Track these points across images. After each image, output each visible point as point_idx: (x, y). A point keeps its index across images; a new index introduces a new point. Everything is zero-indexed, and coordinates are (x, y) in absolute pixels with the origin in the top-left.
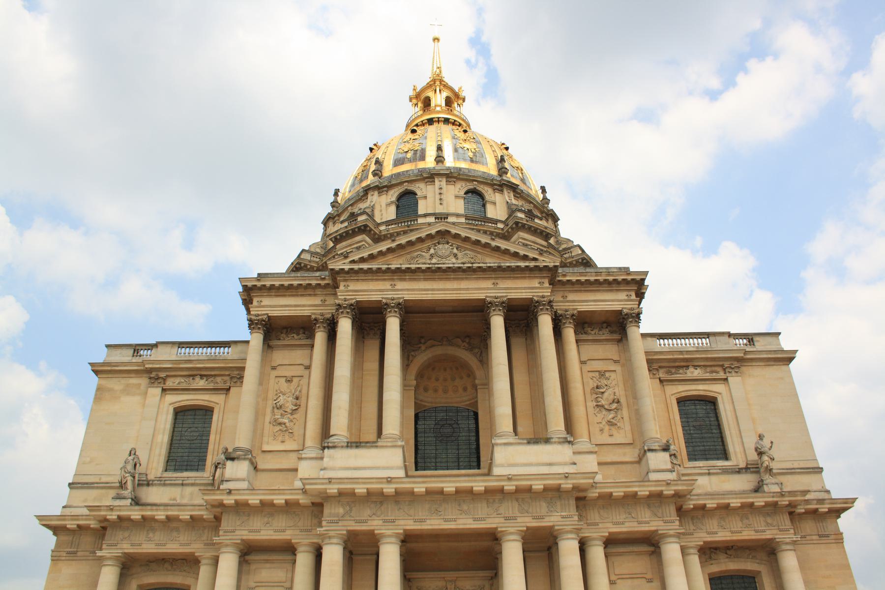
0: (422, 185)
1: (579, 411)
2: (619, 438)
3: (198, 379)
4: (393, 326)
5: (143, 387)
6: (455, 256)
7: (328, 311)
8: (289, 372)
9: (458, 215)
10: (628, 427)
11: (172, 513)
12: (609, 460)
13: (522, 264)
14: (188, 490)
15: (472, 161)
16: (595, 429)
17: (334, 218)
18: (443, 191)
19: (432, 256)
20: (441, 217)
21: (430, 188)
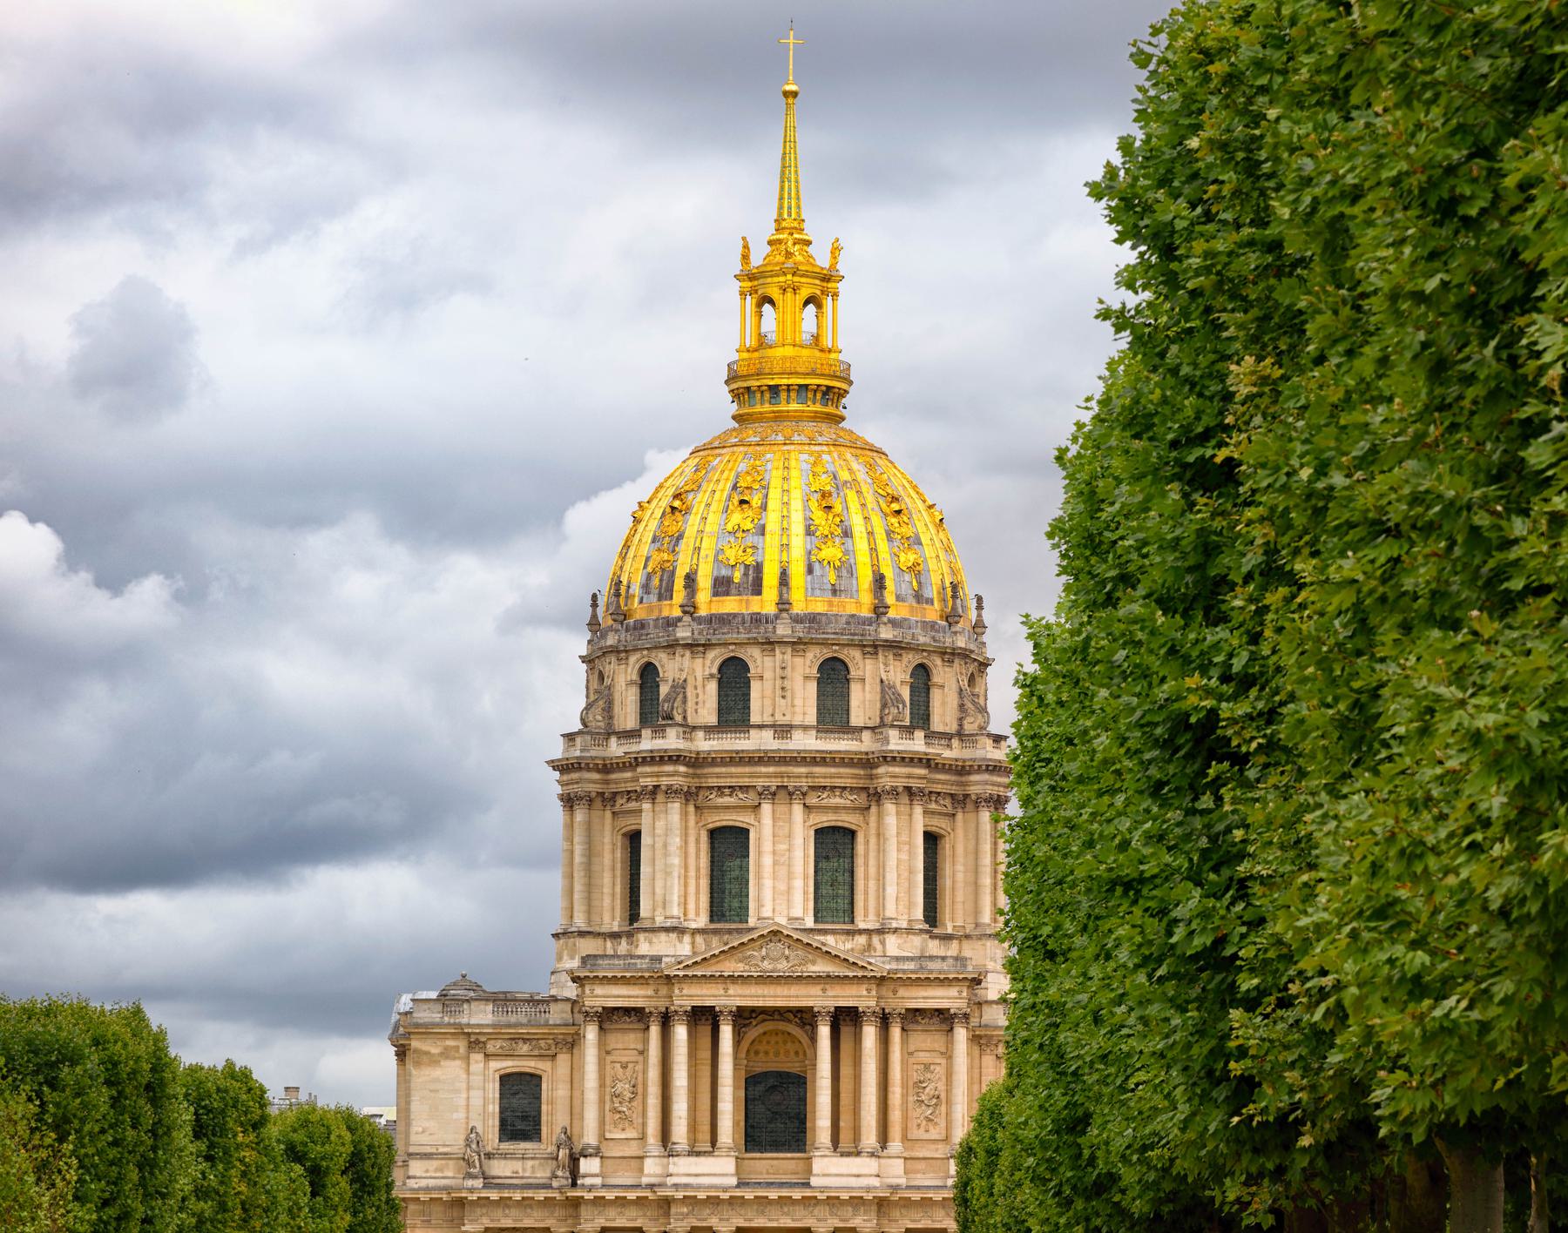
0: (755, 652)
1: (895, 1116)
2: (935, 1133)
3: (521, 1043)
4: (726, 1032)
5: (462, 1050)
6: (787, 958)
7: (662, 1004)
8: (624, 1059)
9: (805, 728)
10: (943, 1124)
11: (528, 1194)
12: (921, 1155)
13: (851, 974)
14: (530, 1163)
15: (835, 591)
16: (912, 1124)
17: (619, 652)
18: (788, 672)
19: (763, 958)
20: (783, 730)
21: (768, 661)
